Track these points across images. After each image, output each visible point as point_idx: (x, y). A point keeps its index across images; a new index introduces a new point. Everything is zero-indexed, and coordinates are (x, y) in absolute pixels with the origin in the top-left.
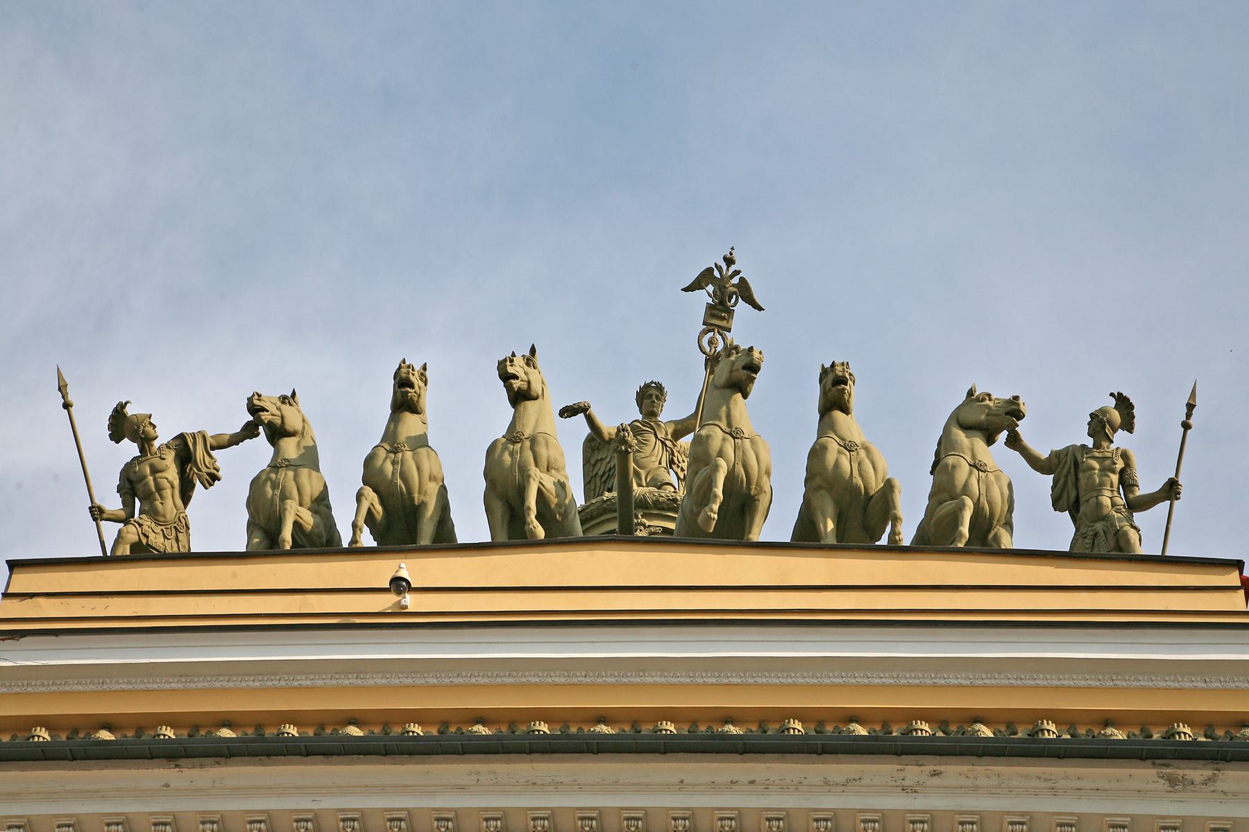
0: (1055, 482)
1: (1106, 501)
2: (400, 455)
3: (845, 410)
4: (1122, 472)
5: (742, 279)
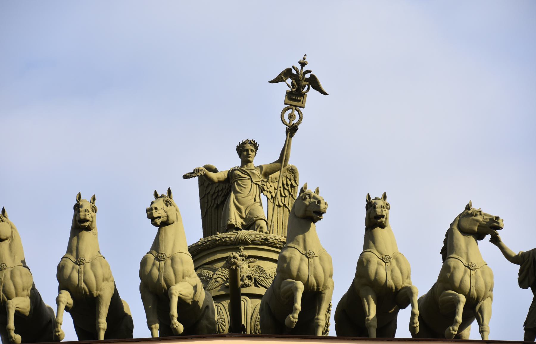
0: (521, 271)
2: (82, 267)
3: (383, 226)
5: (313, 77)
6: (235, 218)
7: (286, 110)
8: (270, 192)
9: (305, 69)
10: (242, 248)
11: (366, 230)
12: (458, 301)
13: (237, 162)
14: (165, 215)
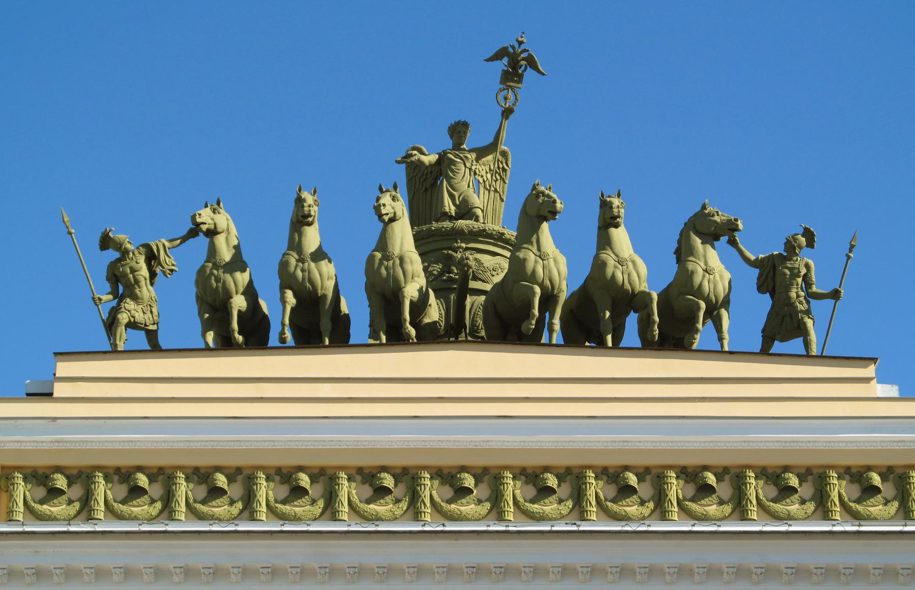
1: (793, 294)
4: (805, 276)
5: (531, 56)
6: (449, 207)
7: (501, 90)
11: (599, 228)
12: (699, 308)
13: (448, 144)
14: (392, 211)
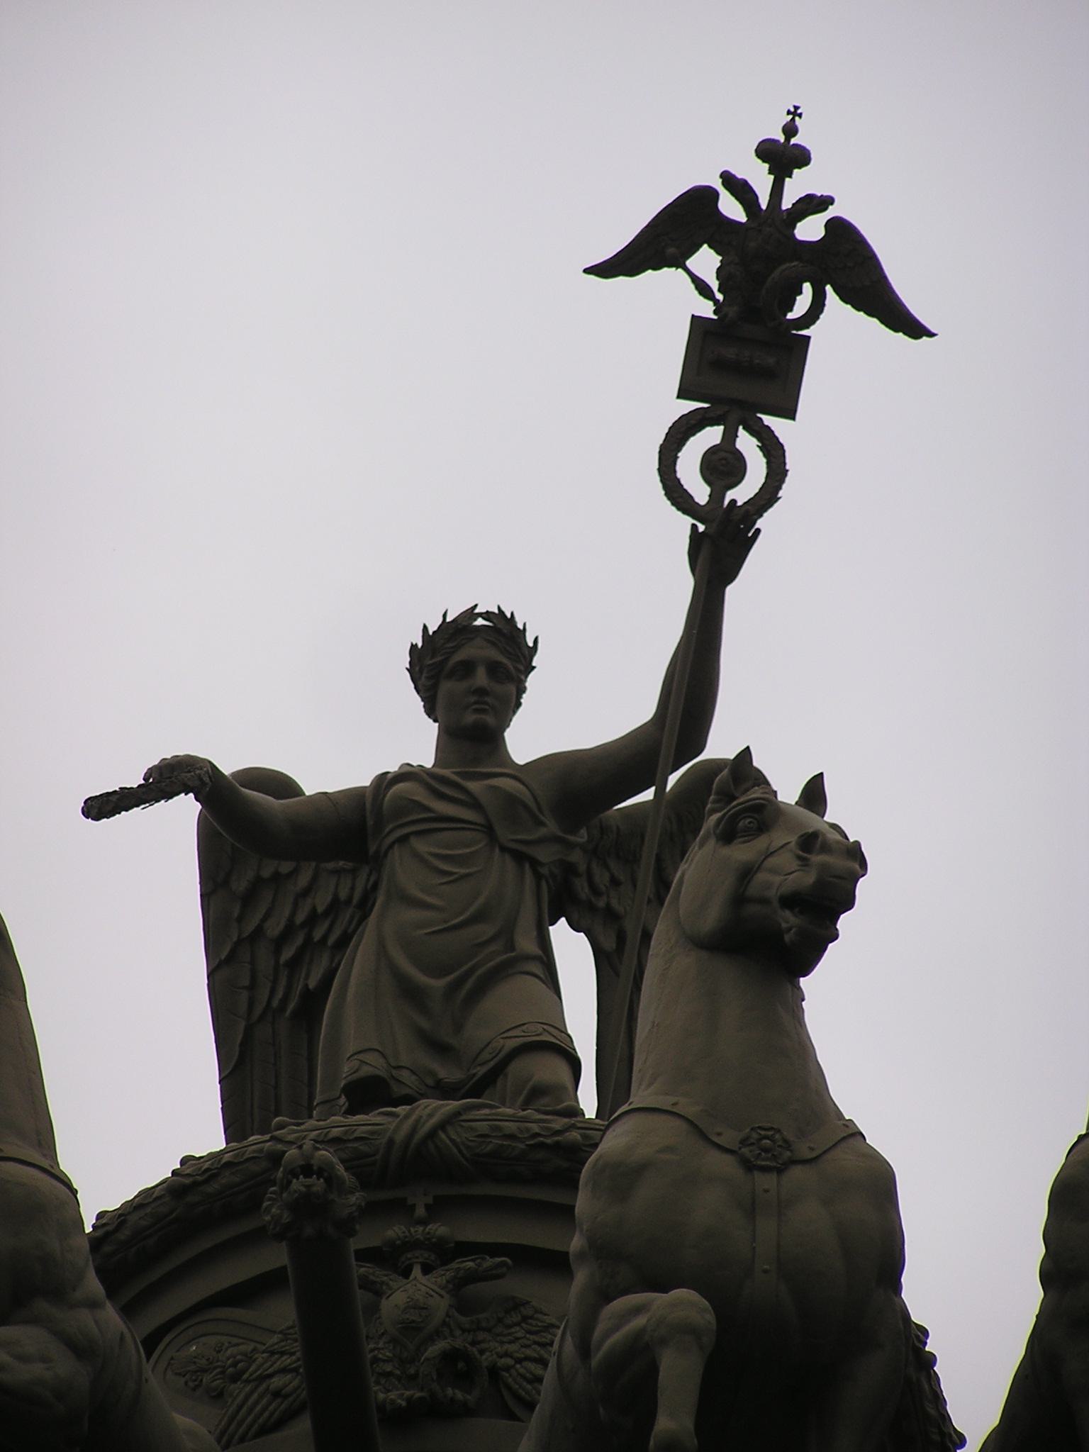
5: (839, 228)
8: (611, 916)
9: (793, 191)
10: (420, 1202)
13: (413, 740)
